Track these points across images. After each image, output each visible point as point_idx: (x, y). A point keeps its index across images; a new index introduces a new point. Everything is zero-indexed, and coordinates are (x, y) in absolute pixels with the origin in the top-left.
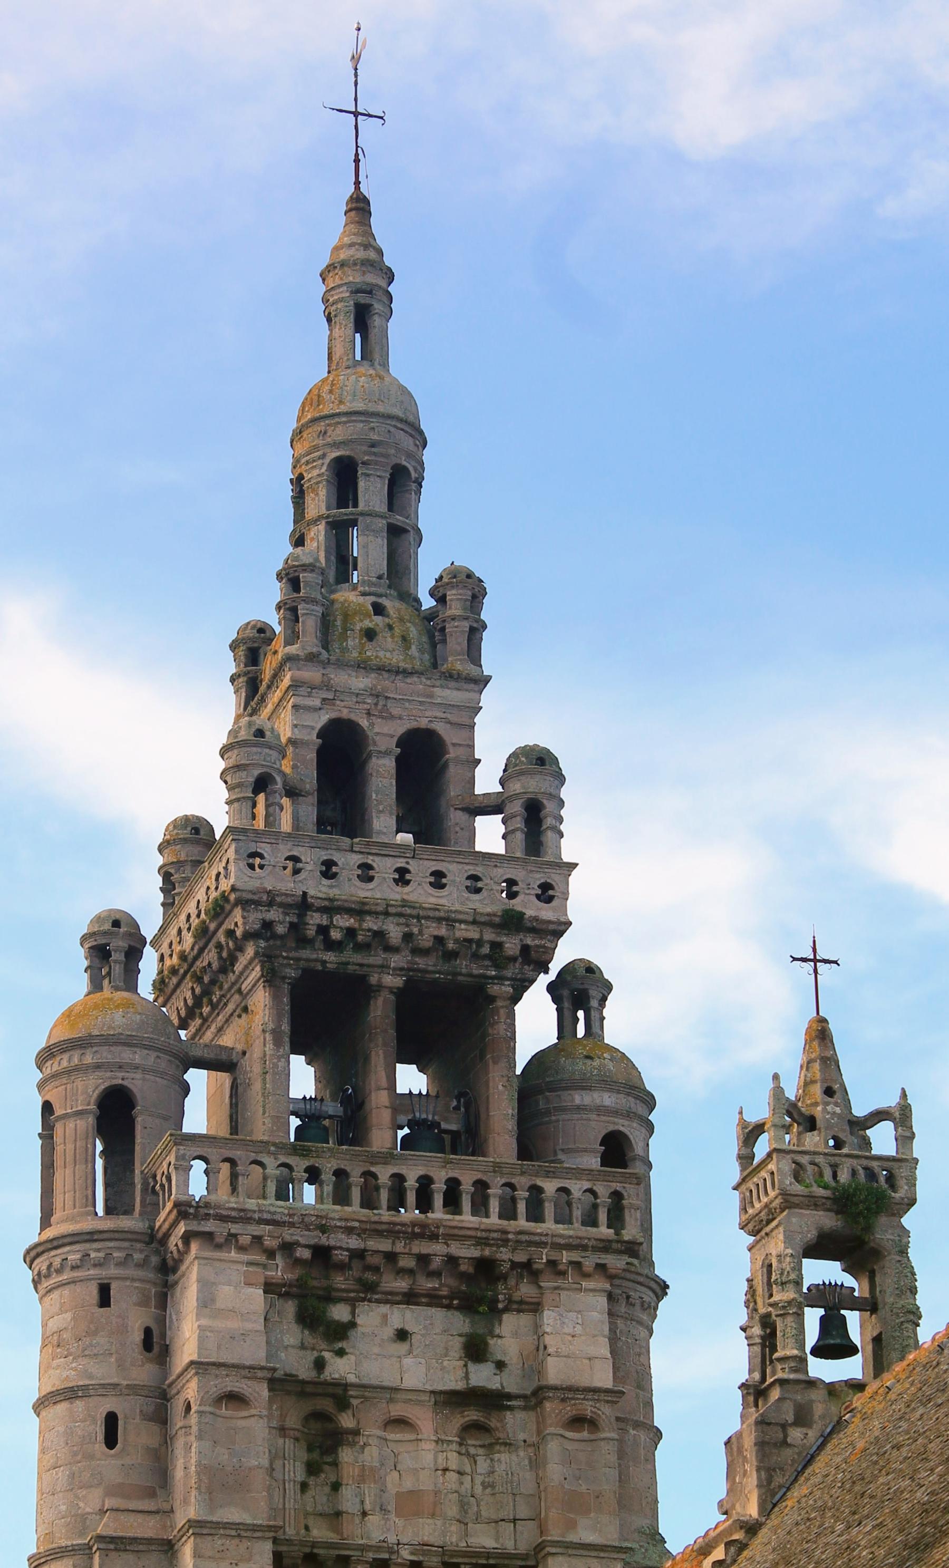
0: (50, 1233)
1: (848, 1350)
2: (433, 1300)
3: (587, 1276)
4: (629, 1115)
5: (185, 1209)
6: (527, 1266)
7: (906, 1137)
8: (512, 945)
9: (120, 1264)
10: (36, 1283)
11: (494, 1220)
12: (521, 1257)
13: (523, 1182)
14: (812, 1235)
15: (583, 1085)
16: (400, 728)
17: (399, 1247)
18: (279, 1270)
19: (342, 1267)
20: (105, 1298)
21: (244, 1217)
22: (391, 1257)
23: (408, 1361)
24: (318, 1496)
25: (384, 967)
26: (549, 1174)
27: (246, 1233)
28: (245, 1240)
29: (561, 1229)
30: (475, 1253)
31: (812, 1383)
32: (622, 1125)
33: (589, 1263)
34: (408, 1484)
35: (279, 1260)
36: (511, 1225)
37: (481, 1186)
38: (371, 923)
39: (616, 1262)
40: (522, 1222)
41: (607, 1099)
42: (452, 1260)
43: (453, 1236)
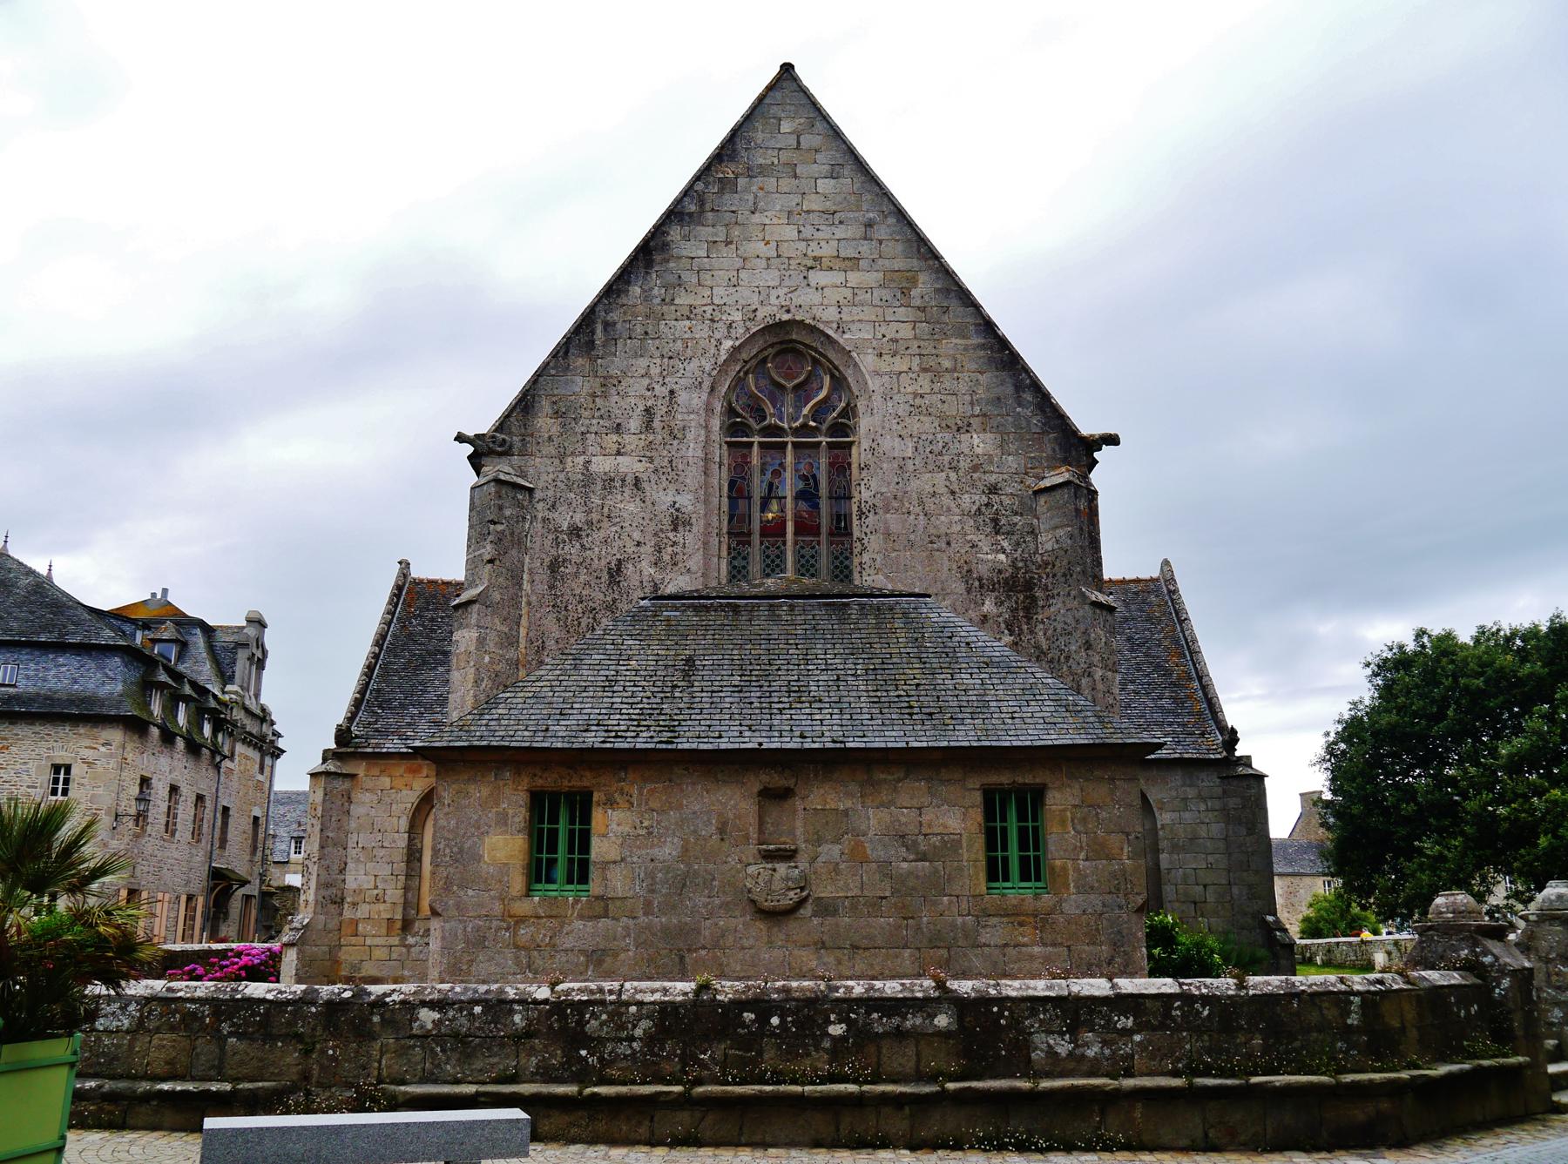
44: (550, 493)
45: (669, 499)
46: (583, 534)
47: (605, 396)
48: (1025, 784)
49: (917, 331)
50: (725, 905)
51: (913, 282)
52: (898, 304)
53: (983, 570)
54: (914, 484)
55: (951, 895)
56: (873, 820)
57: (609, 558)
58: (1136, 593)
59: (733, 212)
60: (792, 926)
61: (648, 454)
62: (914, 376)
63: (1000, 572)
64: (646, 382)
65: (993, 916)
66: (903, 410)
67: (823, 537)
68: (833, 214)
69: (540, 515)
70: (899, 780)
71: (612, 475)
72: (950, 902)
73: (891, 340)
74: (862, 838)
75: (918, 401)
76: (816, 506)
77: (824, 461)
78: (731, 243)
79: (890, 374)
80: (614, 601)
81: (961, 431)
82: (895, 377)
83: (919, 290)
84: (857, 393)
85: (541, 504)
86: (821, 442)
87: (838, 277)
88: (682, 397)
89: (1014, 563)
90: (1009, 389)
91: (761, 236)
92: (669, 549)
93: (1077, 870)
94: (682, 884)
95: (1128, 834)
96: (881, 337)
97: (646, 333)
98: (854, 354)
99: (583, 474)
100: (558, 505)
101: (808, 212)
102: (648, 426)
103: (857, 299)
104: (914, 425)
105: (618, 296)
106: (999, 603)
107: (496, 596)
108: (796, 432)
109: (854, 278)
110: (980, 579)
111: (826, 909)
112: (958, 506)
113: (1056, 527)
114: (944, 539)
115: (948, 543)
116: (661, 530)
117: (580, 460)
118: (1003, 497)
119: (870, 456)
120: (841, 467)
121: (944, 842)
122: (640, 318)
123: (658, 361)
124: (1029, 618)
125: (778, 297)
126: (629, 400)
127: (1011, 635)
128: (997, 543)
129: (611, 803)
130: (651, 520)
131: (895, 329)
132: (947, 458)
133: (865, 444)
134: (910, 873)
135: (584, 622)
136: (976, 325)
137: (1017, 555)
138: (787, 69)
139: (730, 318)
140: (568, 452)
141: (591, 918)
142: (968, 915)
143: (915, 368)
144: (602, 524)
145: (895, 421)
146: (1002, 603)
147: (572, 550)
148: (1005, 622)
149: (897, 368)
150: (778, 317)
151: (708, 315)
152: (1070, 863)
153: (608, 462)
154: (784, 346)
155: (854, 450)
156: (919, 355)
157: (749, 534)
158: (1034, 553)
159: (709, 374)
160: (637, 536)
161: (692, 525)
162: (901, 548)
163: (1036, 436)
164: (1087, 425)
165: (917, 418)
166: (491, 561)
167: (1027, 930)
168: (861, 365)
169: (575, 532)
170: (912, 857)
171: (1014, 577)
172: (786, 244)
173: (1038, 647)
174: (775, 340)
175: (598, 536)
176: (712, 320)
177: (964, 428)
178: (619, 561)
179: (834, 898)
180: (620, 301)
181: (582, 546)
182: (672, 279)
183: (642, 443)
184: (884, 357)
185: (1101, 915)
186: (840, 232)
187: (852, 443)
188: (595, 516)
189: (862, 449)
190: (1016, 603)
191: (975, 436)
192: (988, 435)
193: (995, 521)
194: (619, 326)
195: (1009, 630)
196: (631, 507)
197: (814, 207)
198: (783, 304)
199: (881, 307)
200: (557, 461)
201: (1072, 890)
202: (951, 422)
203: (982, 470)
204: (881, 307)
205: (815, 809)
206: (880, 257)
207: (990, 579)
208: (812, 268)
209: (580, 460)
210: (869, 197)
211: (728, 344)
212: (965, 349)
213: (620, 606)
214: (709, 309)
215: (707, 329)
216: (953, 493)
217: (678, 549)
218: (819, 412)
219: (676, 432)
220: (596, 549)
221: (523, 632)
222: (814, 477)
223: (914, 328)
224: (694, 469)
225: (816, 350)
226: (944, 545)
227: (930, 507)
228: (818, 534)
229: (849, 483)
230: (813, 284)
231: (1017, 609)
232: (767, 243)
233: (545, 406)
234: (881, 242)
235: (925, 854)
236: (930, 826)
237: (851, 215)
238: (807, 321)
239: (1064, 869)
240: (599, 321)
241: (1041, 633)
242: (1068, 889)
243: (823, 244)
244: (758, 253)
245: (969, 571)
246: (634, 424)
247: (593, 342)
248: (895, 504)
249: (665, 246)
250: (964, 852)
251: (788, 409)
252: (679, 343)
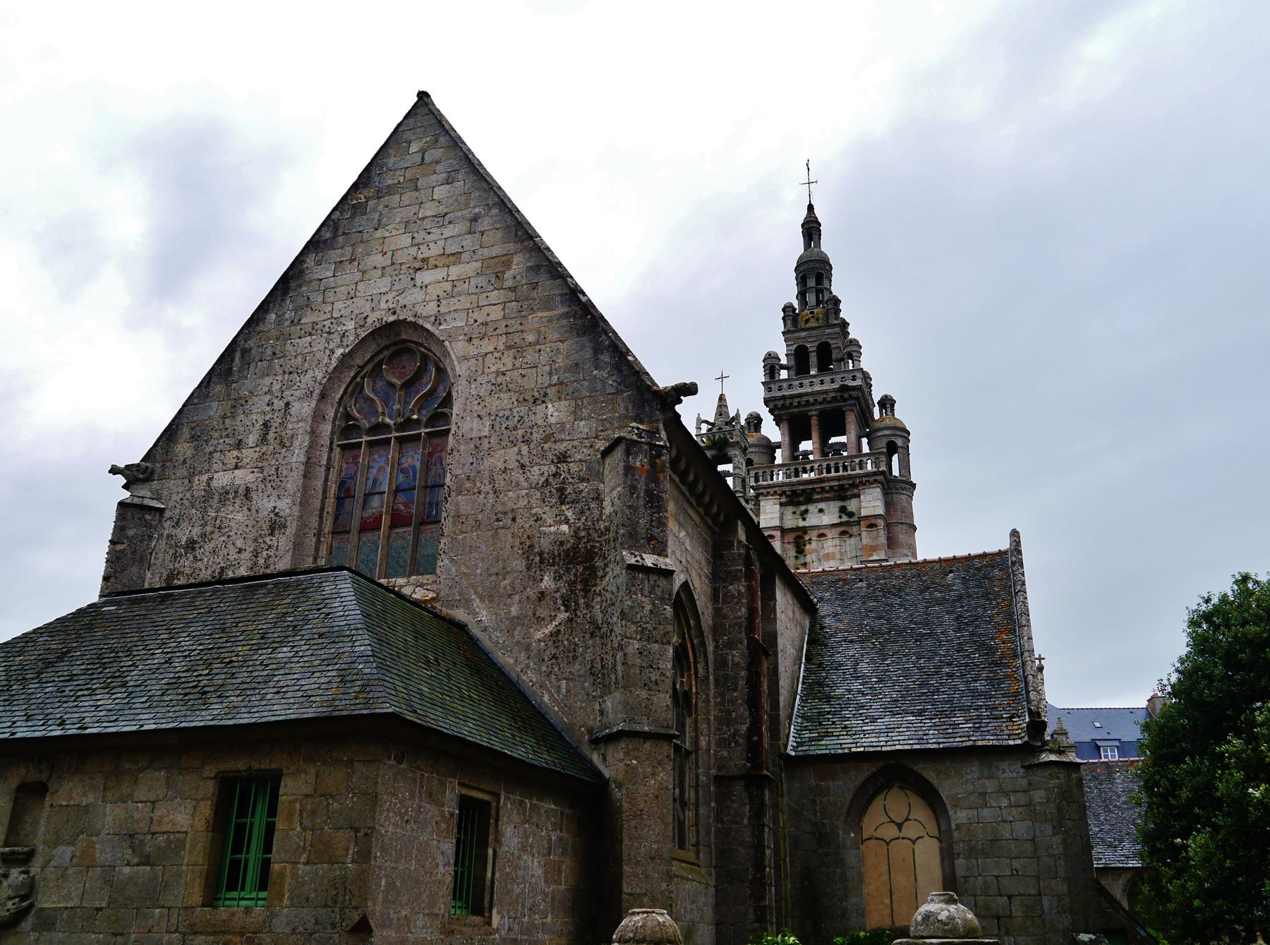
2: (828, 499)
3: (872, 484)
6: (854, 483)
8: (846, 396)
11: (841, 473)
12: (851, 482)
16: (816, 344)
17: (815, 486)
18: (783, 500)
19: (800, 495)
22: (814, 489)
23: (824, 517)
24: (802, 560)
25: (812, 410)
28: (772, 493)
30: (837, 483)
32: (893, 439)
33: (871, 479)
34: (826, 552)
38: (805, 399)
41: (887, 432)
42: (831, 487)
43: (830, 479)
44: (177, 511)
45: (271, 505)
47: (233, 416)
48: (261, 770)
49: (507, 311)
51: (508, 265)
52: (492, 288)
53: (545, 544)
54: (488, 463)
55: (163, 907)
56: (111, 815)
57: (215, 567)
58: (979, 569)
59: (360, 232)
61: (260, 465)
63: (562, 543)
64: (267, 398)
65: (201, 933)
68: (444, 216)
70: (142, 770)
71: (228, 488)
72: (161, 916)
73: (482, 324)
74: (94, 838)
75: (500, 379)
78: (355, 260)
79: (476, 357)
81: (538, 402)
82: (480, 359)
83: (512, 272)
85: (168, 522)
87: (439, 274)
88: (294, 409)
90: (588, 353)
91: (380, 249)
92: (265, 553)
93: (294, 875)
95: (357, 830)
96: (472, 321)
97: (274, 354)
98: (447, 343)
99: (205, 490)
100: (181, 521)
101: (423, 219)
102: (264, 439)
103: (456, 290)
105: (257, 325)
106: (557, 578)
108: (400, 427)
109: (455, 272)
112: (527, 480)
115: (514, 520)
116: (261, 535)
117: (205, 478)
118: (571, 464)
121: (169, 842)
122: (271, 342)
124: (586, 591)
125: (387, 301)
126: (252, 416)
127: (566, 611)
128: (561, 513)
130: (253, 526)
131: (485, 314)
132: (520, 432)
134: (130, 879)
136: (561, 295)
138: (423, 96)
139: (345, 328)
140: (196, 472)
142: (176, 931)
143: (501, 347)
144: (214, 536)
145: (476, 402)
146: (561, 577)
148: (562, 597)
149: (484, 351)
150: (385, 319)
151: (327, 329)
152: (289, 867)
153: (227, 476)
154: (398, 347)
156: (506, 334)
158: (598, 520)
159: (320, 383)
160: (239, 543)
162: (469, 529)
163: (610, 397)
164: (664, 379)
165: (497, 396)
168: (451, 352)
169: (191, 545)
170: (136, 860)
171: (575, 547)
172: (400, 252)
173: (593, 622)
174: (388, 343)
175: (209, 547)
176: (329, 333)
178: (222, 569)
179: (55, 909)
180: (258, 329)
181: (195, 557)
182: (301, 301)
183: (256, 455)
184: (475, 341)
185: (311, 934)
186: (448, 232)
190: (575, 575)
191: (550, 406)
192: (563, 403)
193: (561, 490)
195: (565, 605)
196: (239, 517)
197: (429, 213)
198: (391, 307)
199: (475, 294)
200: (186, 481)
201: (286, 901)
202: (528, 396)
203: (553, 439)
204: (475, 294)
205: (61, 806)
206: (481, 247)
207: (551, 553)
208: (420, 269)
209: (205, 478)
210: (477, 194)
211: (340, 351)
212: (550, 321)
214: (327, 323)
215: (324, 341)
216: (523, 466)
217: (271, 553)
219: (285, 440)
220: (206, 560)
223: (504, 309)
226: (509, 522)
227: (500, 483)
230: (419, 284)
231: (575, 582)
232: (385, 254)
233: (185, 432)
234: (482, 233)
235: (148, 856)
236: (160, 822)
237: (459, 214)
238: (409, 320)
239: (282, 874)
240: (239, 349)
241: (598, 607)
242: (281, 900)
243: (432, 245)
244: (375, 264)
245: (532, 546)
246: (252, 439)
248: (468, 485)
249: (302, 272)
252: (300, 359)
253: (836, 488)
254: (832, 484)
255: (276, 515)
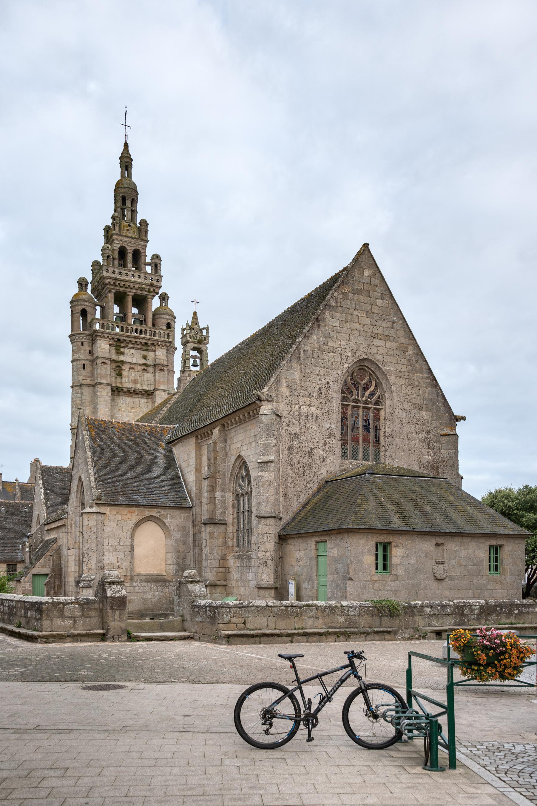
0: (73, 333)
1: (197, 366)
2: (137, 349)
4: (171, 320)
5: (95, 331)
6: (153, 344)
7: (208, 333)
9: (85, 339)
10: (71, 341)
11: (148, 336)
12: (152, 342)
13: (153, 330)
14: (192, 347)
15: (164, 314)
20: (82, 345)
21: (106, 333)
22: (131, 341)
26: (157, 329)
27: (106, 335)
29: (159, 338)
31: (191, 371)
32: (170, 321)
33: (164, 344)
35: (112, 341)
36: (150, 337)
37: (146, 330)
39: (168, 345)
40: (153, 337)
42: (141, 342)
45: (328, 426)
46: (299, 436)
50: (427, 577)
53: (424, 462)
54: (405, 428)
56: (463, 553)
60: (444, 583)
62: (406, 387)
64: (319, 377)
66: (402, 399)
67: (372, 444)
69: (284, 428)
75: (407, 397)
76: (369, 431)
77: (372, 415)
80: (310, 463)
84: (385, 390)
86: (371, 407)
88: (332, 385)
89: (433, 461)
92: (328, 445)
94: (416, 571)
104: (406, 406)
107: (276, 460)
110: (423, 465)
111: (452, 579)
113: (449, 449)
114: (413, 449)
117: (297, 407)
119: (390, 416)
120: (377, 418)
123: (323, 369)
129: (397, 546)
132: (415, 419)
133: (388, 410)
135: (301, 470)
137: (434, 457)
141: (393, 581)
147: (296, 443)
155: (382, 412)
157: (347, 440)
160: (317, 439)
161: (335, 436)
164: (457, 412)
166: (274, 446)
167: (498, 585)
169: (296, 435)
171: (433, 465)
175: (305, 438)
176: (341, 354)
177: (420, 409)
178: (312, 449)
181: (299, 441)
187: (381, 409)
188: (303, 430)
189: (387, 412)
194: (309, 352)
196: (315, 427)
200: (289, 406)
202: (417, 406)
209: (297, 407)
211: (346, 365)
213: (312, 465)
216: (417, 433)
217: (331, 445)
218: (372, 395)
221: (281, 473)
222: (368, 420)
224: (335, 414)
225: (372, 370)
228: (370, 443)
229: (379, 423)
239: (507, 568)
245: (420, 462)
246: (315, 394)
247: (299, 358)
250: (484, 563)
251: (360, 392)
253: (144, 344)
254: (142, 341)
255: (331, 430)
